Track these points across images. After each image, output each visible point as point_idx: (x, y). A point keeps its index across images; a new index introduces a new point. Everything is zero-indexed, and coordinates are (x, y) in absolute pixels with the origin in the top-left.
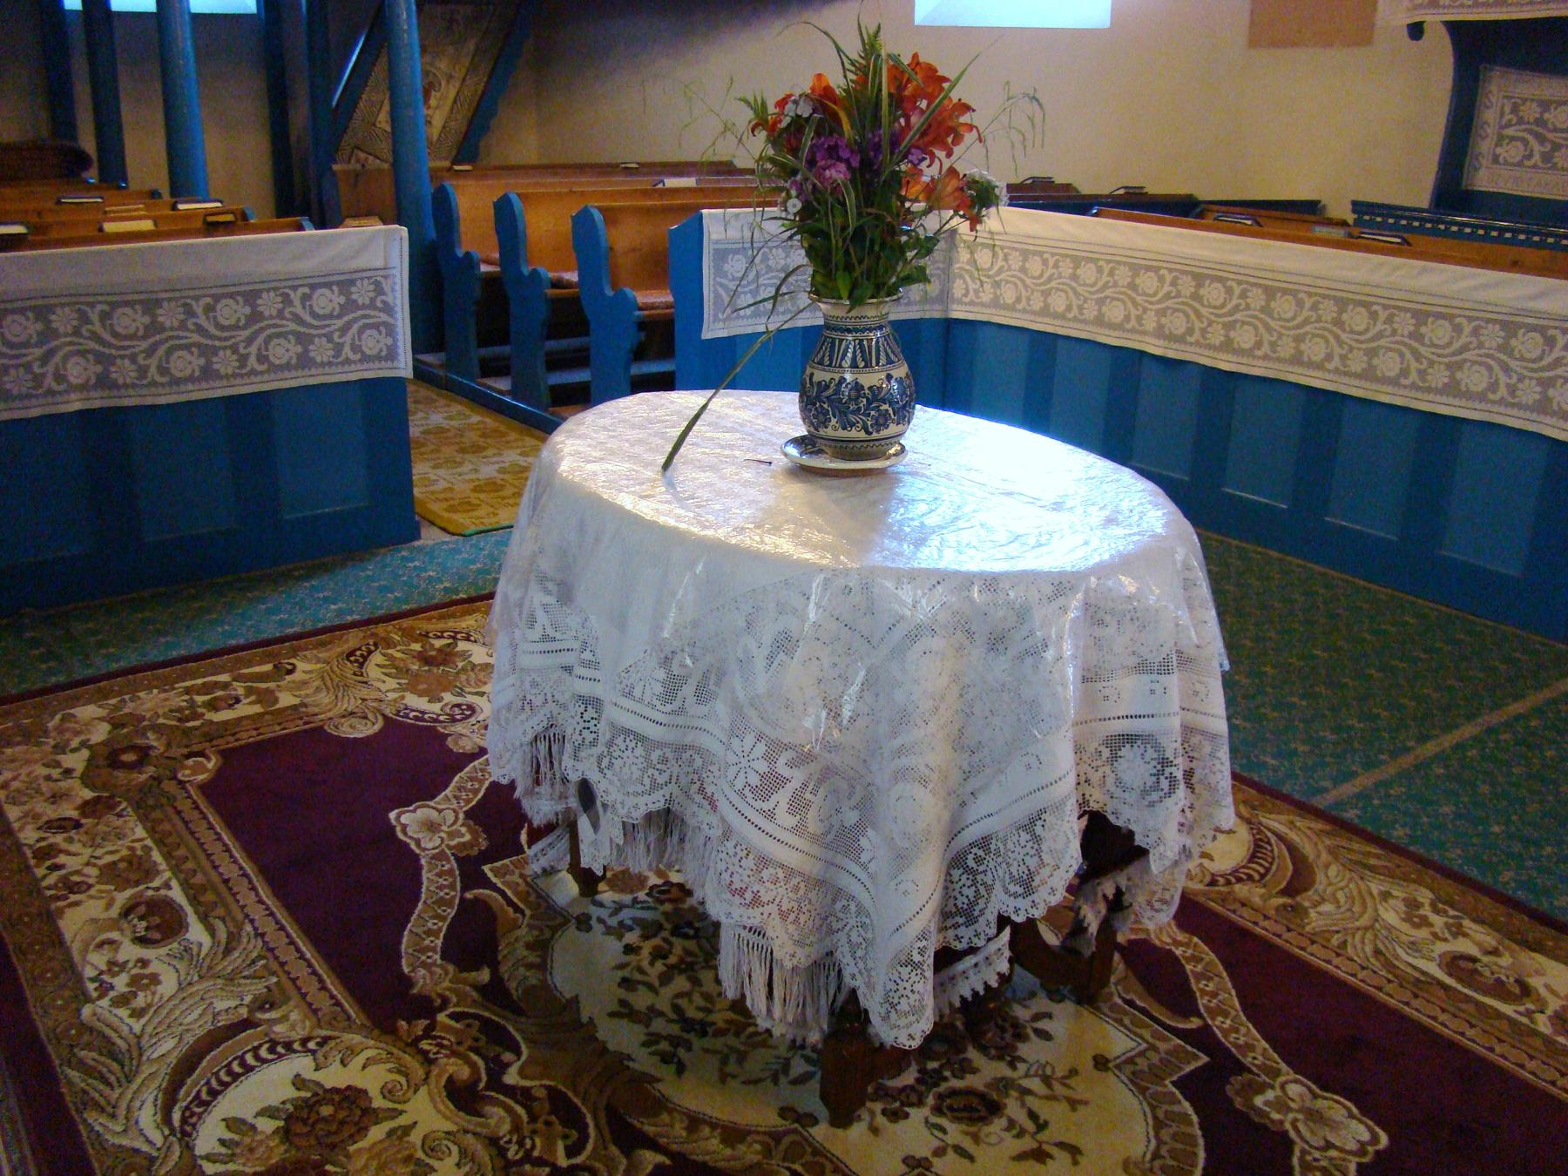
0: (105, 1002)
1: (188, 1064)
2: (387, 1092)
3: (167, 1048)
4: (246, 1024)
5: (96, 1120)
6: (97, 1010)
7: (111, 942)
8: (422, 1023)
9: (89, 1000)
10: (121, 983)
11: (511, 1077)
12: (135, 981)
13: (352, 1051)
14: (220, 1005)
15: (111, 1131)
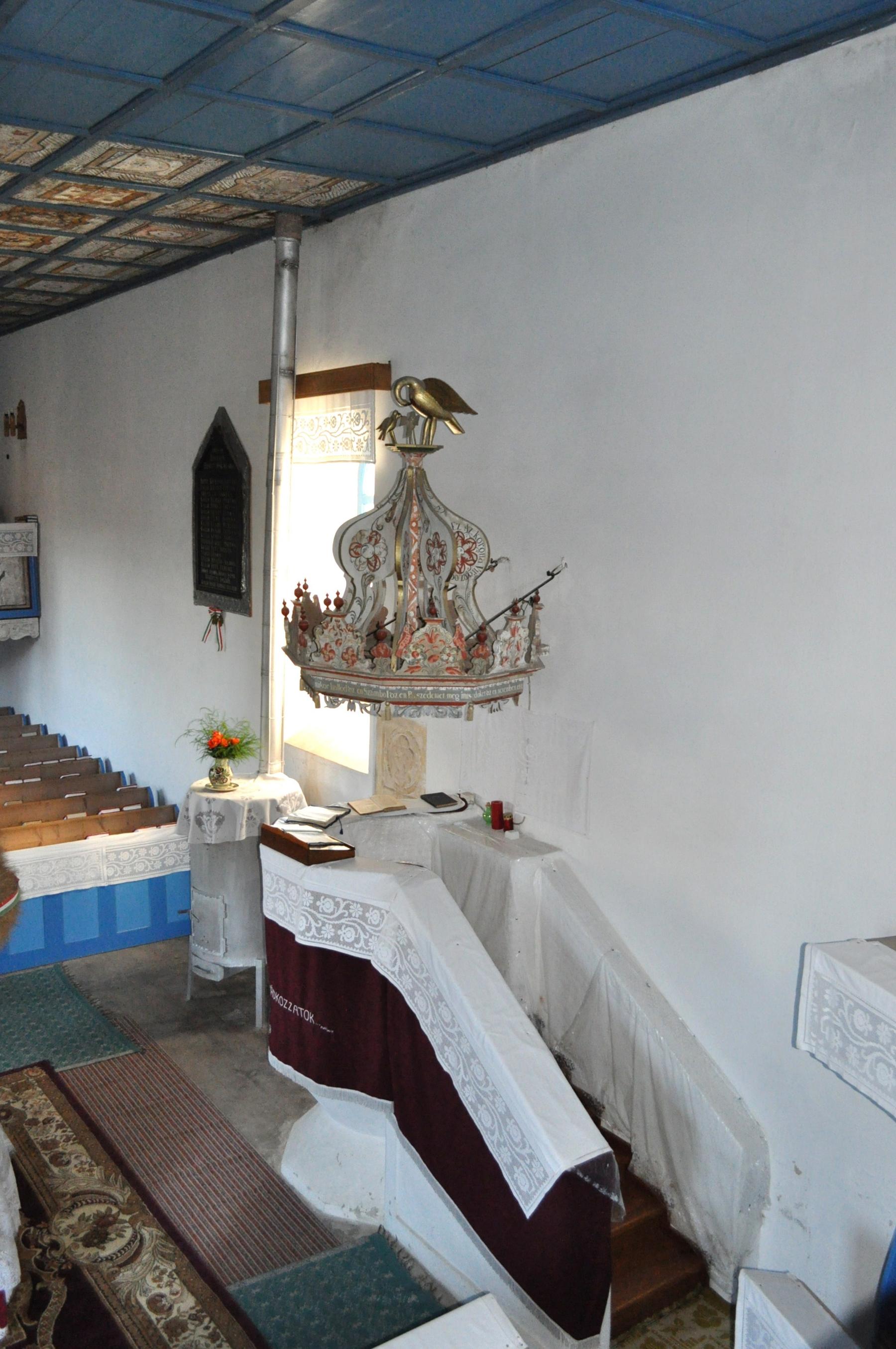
0: (169, 1270)
1: (137, 1253)
2: (77, 1247)
3: (145, 1257)
4: (120, 1266)
5: (160, 1234)
6: (170, 1267)
7: (173, 1294)
8: (64, 1268)
9: (174, 1270)
10: (166, 1278)
11: (39, 1251)
12: (161, 1279)
13: (87, 1258)
14: (130, 1272)
15: (155, 1231)
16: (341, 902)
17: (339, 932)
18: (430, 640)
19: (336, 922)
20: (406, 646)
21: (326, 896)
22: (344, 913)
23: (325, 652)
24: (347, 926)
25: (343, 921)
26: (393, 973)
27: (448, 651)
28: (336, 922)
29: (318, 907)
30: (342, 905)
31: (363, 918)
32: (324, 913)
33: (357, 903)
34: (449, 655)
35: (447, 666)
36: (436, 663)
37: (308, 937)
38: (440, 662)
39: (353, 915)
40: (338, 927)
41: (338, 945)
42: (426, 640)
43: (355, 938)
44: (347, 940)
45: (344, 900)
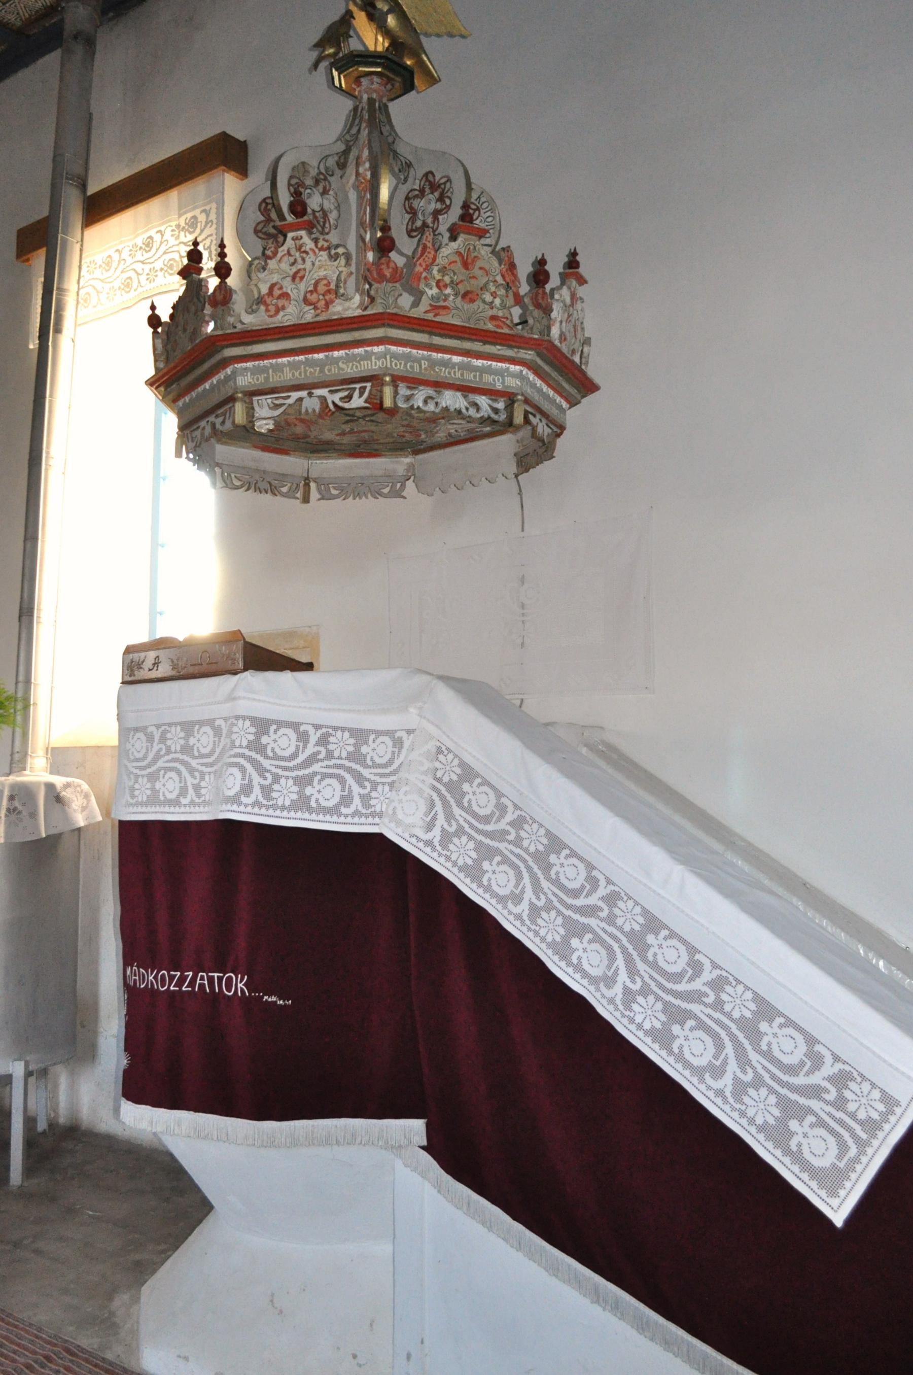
16: (311, 731)
17: (308, 791)
18: (466, 265)
19: (300, 773)
20: (428, 268)
21: (281, 724)
22: (319, 752)
23: (268, 300)
24: (325, 776)
25: (316, 767)
26: (429, 843)
27: (493, 288)
28: (300, 773)
29: (265, 747)
30: (314, 738)
31: (356, 756)
32: (276, 757)
33: (343, 729)
34: (494, 295)
35: (491, 313)
36: (474, 306)
37: (246, 806)
38: (482, 305)
39: (336, 754)
40: (303, 782)
41: (306, 816)
42: (459, 264)
43: (342, 797)
44: (324, 803)
45: (317, 727)
